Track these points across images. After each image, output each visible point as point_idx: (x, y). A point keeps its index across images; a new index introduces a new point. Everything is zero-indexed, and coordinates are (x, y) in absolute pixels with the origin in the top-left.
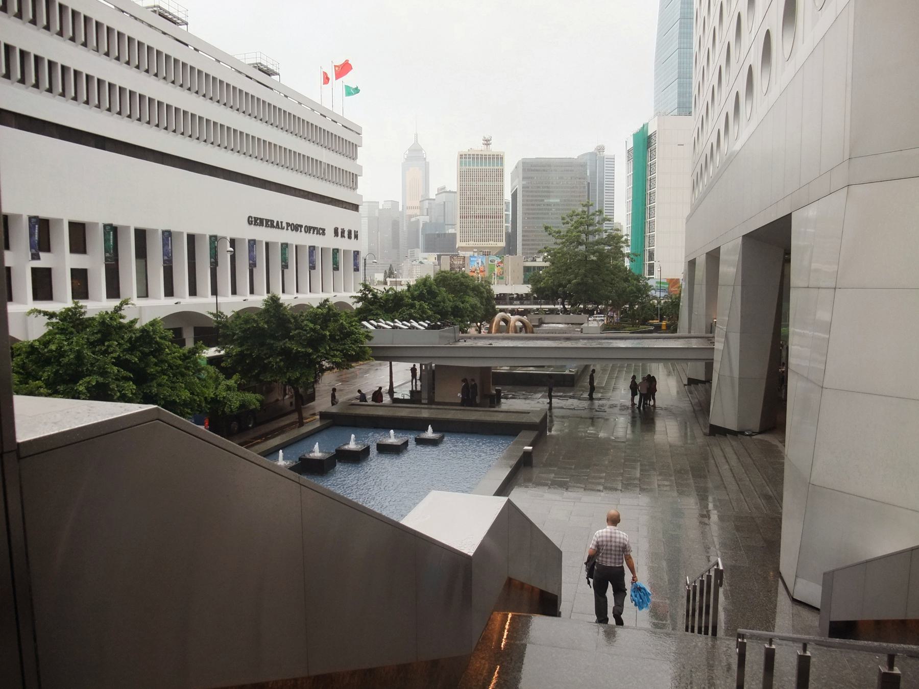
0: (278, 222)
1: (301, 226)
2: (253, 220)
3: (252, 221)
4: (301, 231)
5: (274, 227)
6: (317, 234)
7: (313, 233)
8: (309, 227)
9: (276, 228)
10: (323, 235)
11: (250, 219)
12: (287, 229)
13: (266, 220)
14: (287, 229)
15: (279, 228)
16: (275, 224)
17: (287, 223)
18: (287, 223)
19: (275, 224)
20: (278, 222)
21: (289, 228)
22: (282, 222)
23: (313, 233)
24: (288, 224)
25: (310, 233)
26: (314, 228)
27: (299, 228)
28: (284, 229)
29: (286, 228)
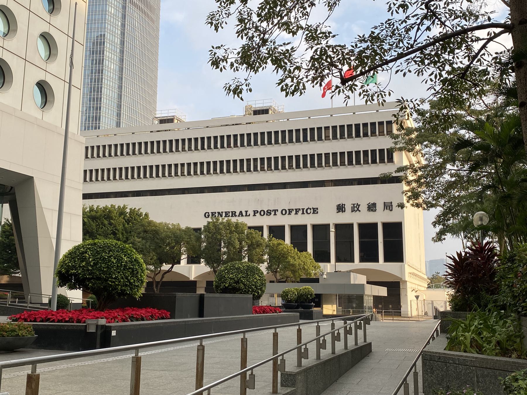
0: (241, 212)
1: (275, 211)
2: (210, 214)
3: (209, 216)
4: (275, 214)
5: (235, 216)
6: (303, 213)
7: (296, 214)
8: (289, 210)
9: (239, 216)
10: (314, 213)
11: (207, 214)
12: (254, 215)
13: (226, 212)
14: (254, 215)
15: (242, 216)
16: (237, 214)
17: (254, 211)
18: (254, 211)
19: (237, 214)
20: (241, 212)
21: (258, 215)
22: (246, 212)
23: (296, 214)
24: (255, 212)
25: (289, 214)
26: (297, 211)
27: (273, 213)
28: (249, 215)
29: (252, 214)
